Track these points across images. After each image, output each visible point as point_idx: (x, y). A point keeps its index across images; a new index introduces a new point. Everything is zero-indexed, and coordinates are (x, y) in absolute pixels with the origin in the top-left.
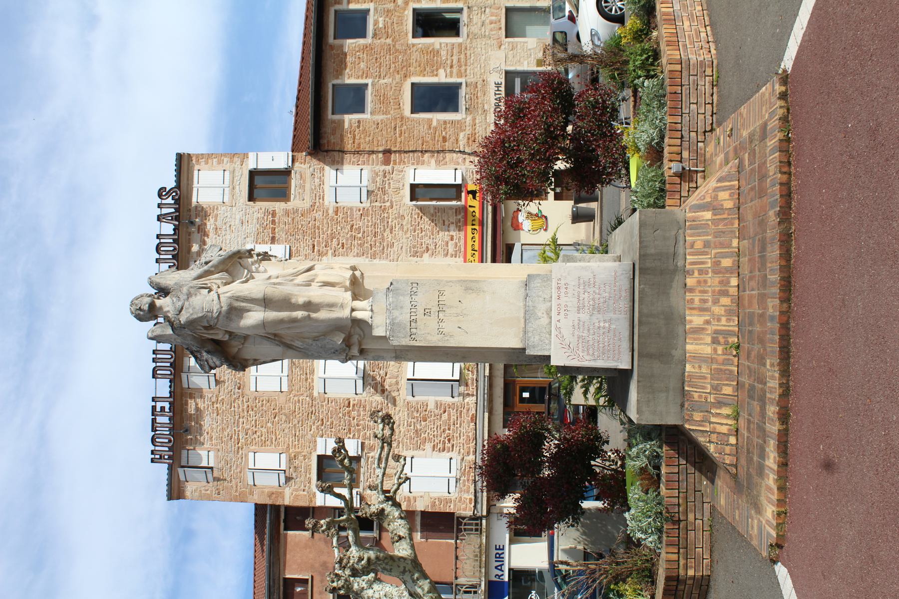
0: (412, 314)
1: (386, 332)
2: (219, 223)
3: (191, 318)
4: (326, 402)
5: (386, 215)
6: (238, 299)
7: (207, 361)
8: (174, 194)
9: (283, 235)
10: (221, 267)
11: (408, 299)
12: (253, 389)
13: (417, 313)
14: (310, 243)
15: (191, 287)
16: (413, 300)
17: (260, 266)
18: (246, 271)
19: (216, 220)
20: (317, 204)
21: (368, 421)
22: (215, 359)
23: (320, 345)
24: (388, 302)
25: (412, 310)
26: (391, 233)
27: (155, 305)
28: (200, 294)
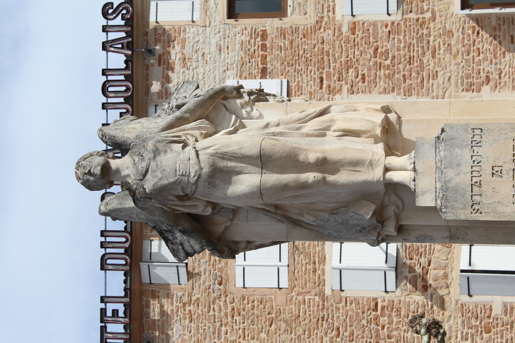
0: (475, 174)
1: (436, 200)
2: (187, 51)
3: (159, 184)
4: (343, 303)
5: (425, 31)
6: (224, 156)
7: (181, 244)
8: (124, 12)
9: (278, 66)
10: (198, 113)
11: (467, 153)
12: (239, 284)
13: (482, 173)
14: (317, 76)
15: (159, 141)
16: (475, 153)
17: (252, 110)
18: (234, 116)
19: (183, 47)
20: (326, 19)
21: (404, 331)
22: (193, 242)
23: (340, 221)
24: (438, 158)
25: (474, 169)
26: (434, 57)
27: (110, 168)
28: (171, 150)
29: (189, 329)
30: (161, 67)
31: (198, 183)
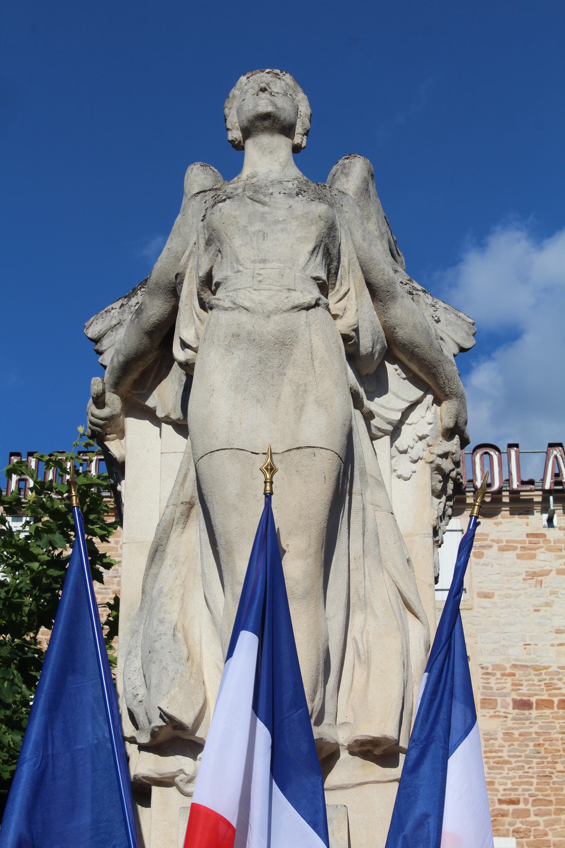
2: (552, 580)
9: (535, 728)
29: (104, 591)
30: (525, 538)
31: (236, 312)
